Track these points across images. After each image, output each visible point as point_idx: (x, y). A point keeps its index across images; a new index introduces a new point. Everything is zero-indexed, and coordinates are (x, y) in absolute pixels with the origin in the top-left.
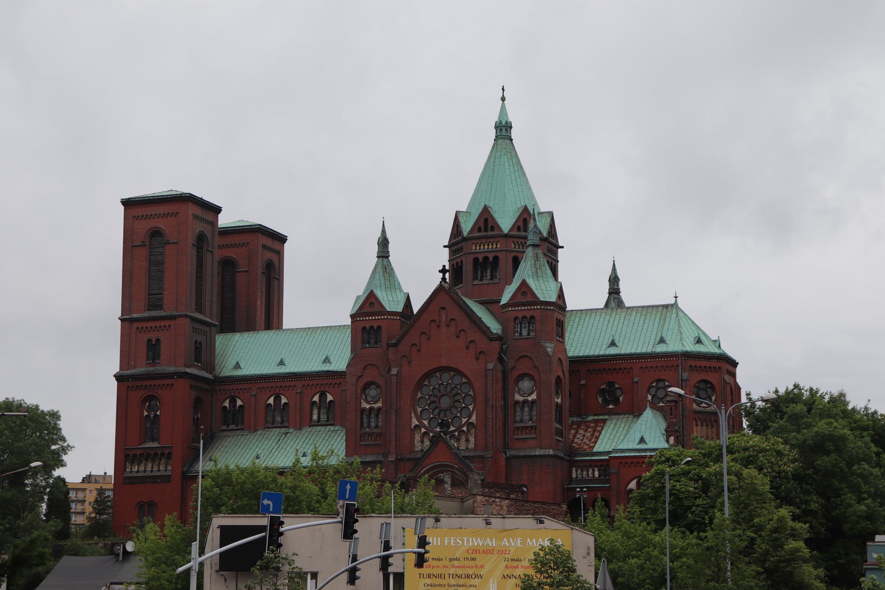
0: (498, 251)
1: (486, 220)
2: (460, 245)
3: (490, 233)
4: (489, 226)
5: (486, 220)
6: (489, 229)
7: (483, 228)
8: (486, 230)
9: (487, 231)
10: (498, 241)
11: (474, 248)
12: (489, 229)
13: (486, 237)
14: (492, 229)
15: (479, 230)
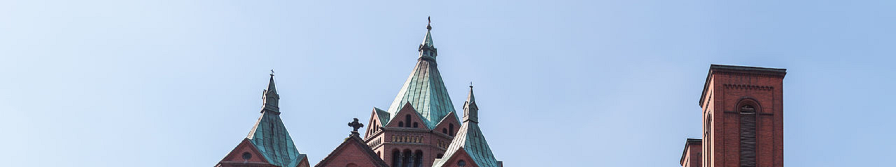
0: (422, 146)
1: (408, 117)
2: (378, 137)
3: (412, 128)
4: (412, 122)
5: (408, 117)
6: (412, 125)
7: (404, 122)
8: (408, 125)
9: (410, 126)
10: (422, 137)
11: (394, 141)
12: (412, 125)
13: (407, 132)
14: (416, 125)
15: (401, 124)
